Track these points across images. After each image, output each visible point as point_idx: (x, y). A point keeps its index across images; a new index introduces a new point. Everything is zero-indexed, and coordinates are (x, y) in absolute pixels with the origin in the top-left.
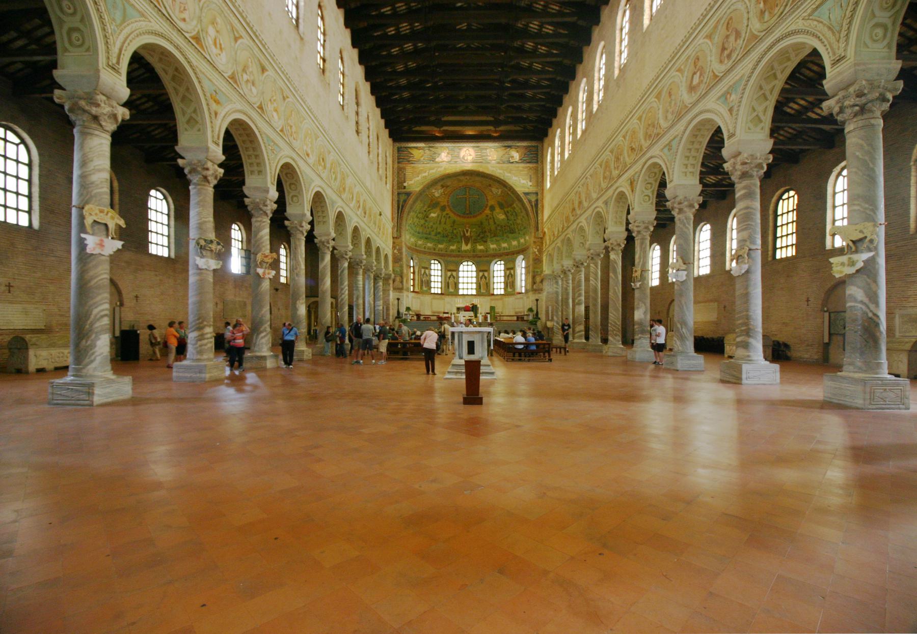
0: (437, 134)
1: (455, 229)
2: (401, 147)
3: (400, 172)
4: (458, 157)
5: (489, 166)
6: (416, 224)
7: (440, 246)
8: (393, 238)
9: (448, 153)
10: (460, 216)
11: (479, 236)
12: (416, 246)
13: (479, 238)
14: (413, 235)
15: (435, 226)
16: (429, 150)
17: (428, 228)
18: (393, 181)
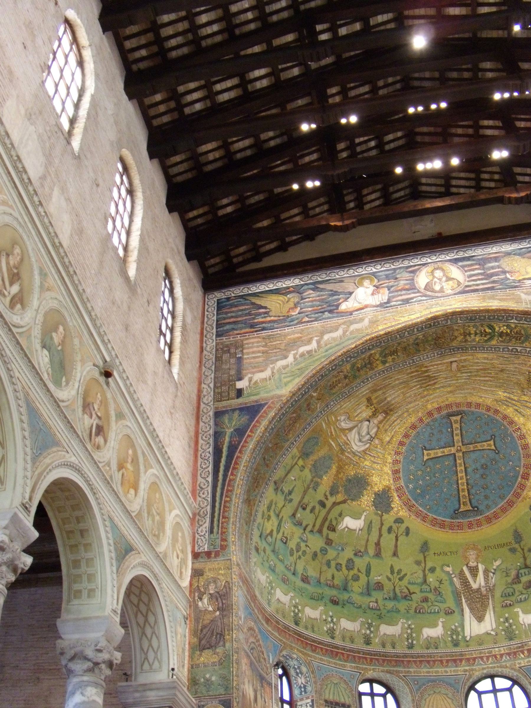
0: (332, 224)
1: (433, 570)
2: (228, 299)
3: (226, 356)
4: (413, 288)
5: (517, 292)
6: (292, 544)
7: (385, 629)
8: (196, 556)
9: (377, 287)
10: (442, 525)
11: (517, 579)
12: (297, 624)
13: (519, 587)
14: (285, 581)
15: (360, 563)
16: (315, 289)
17: (338, 567)
18: (200, 384)
